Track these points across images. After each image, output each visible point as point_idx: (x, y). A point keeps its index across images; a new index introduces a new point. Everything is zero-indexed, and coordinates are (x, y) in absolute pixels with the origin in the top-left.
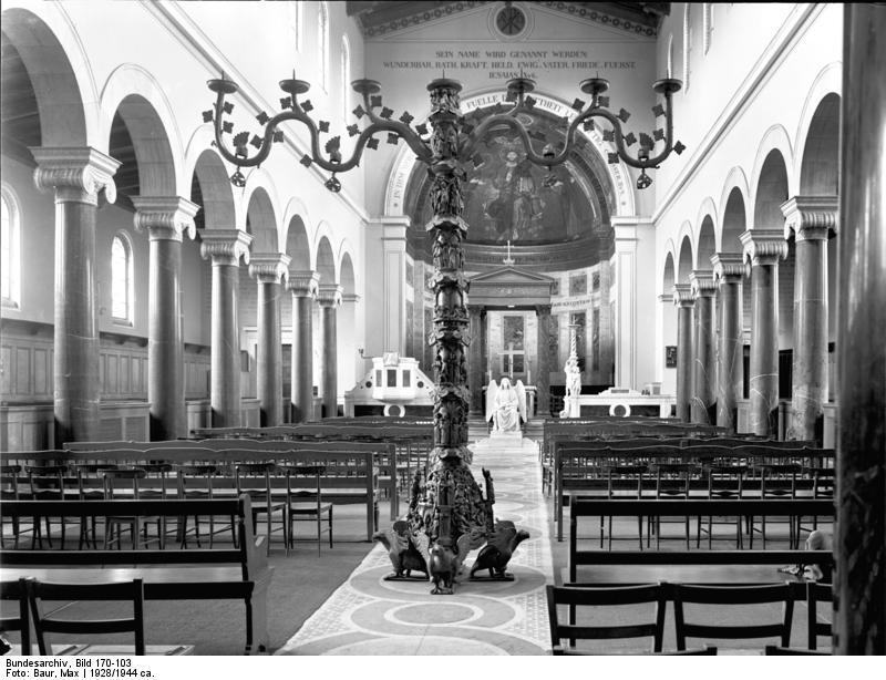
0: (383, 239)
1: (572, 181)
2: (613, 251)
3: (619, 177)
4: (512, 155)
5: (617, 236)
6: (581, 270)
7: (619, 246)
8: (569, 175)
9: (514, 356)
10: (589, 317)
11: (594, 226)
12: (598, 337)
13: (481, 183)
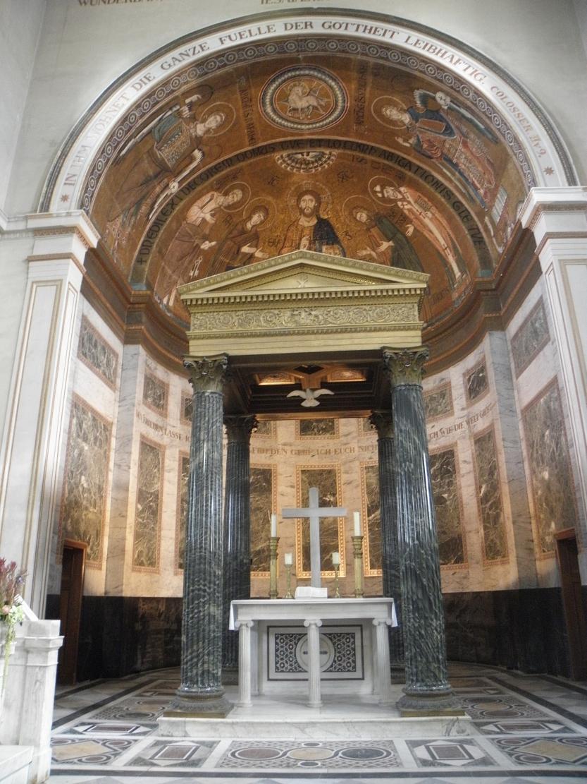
0: (30, 259)
1: (411, 230)
2: (536, 272)
3: (529, 128)
4: (308, 202)
5: (539, 236)
6: (437, 377)
7: (547, 256)
8: (405, 219)
9: (322, 520)
10: (465, 455)
11: (455, 295)
12: (494, 487)
13: (258, 254)
